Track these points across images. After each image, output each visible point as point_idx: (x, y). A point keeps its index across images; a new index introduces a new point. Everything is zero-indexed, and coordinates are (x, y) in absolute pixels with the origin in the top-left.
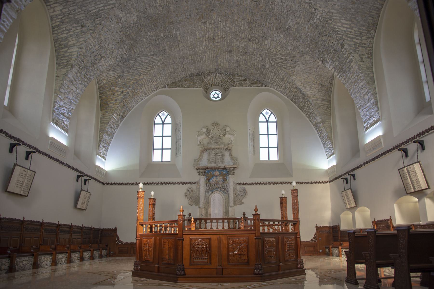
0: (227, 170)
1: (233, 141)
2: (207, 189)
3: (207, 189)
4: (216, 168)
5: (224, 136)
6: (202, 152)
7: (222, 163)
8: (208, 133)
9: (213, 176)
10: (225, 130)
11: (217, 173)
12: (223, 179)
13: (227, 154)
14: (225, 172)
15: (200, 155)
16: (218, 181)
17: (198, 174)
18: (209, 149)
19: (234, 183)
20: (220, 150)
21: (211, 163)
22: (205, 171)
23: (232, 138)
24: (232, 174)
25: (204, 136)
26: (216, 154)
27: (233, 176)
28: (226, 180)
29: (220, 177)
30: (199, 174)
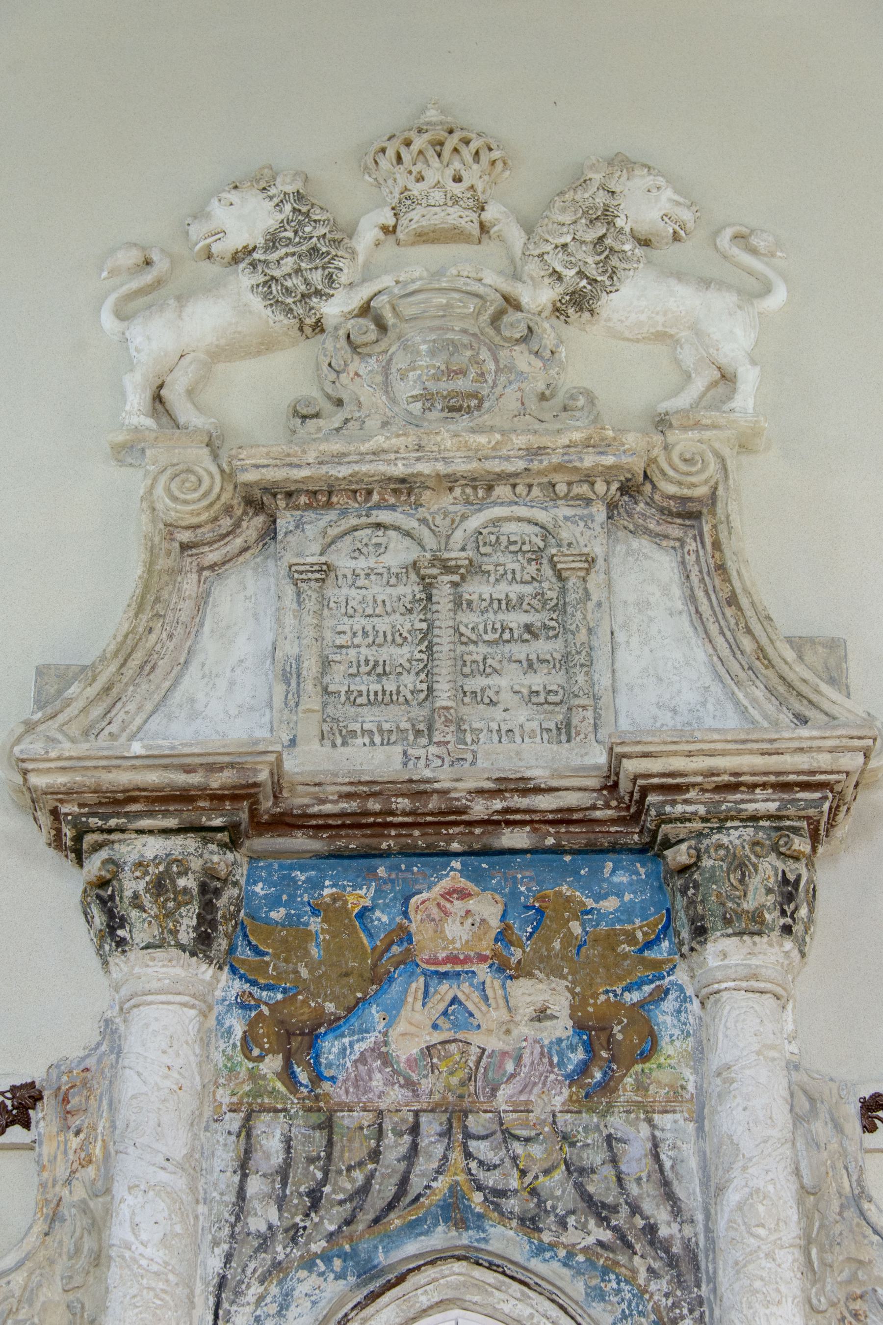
0: (652, 847)
1: (749, 378)
2: (263, 1216)
3: (263, 1216)
4: (452, 816)
5: (579, 302)
6: (187, 552)
7: (565, 731)
8: (298, 257)
9: (383, 967)
10: (607, 216)
11: (456, 914)
12: (592, 1030)
13: (644, 579)
14: (619, 891)
15: (150, 601)
16: (484, 1073)
17: (79, 934)
18: (320, 496)
19: (806, 1103)
20: (515, 517)
21: (336, 733)
22: (219, 859)
23: (732, 334)
24: (753, 926)
25: (228, 309)
26: (433, 575)
27: (770, 954)
28: (648, 1046)
29: (528, 993)
30: (113, 931)
